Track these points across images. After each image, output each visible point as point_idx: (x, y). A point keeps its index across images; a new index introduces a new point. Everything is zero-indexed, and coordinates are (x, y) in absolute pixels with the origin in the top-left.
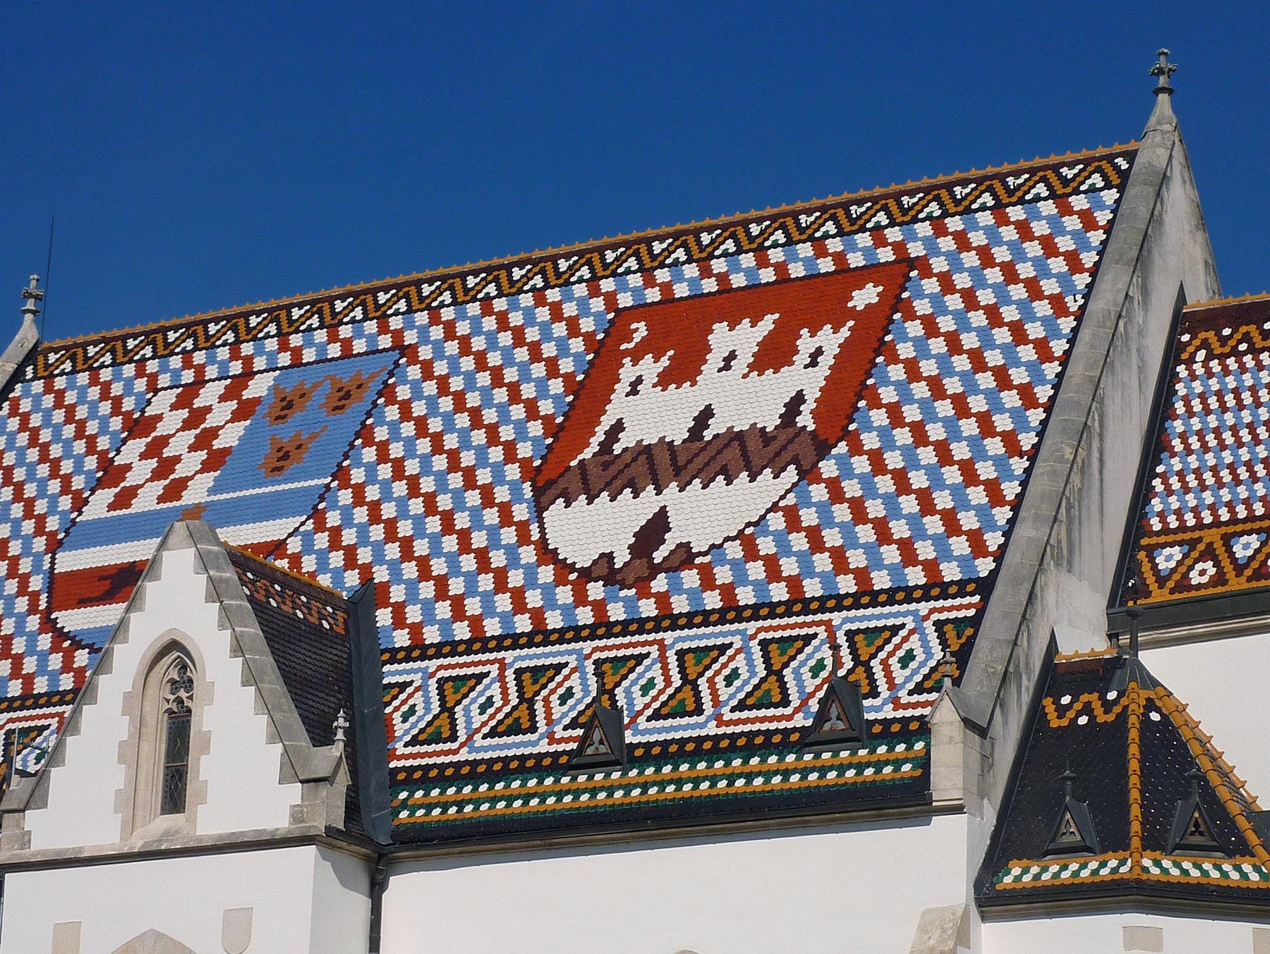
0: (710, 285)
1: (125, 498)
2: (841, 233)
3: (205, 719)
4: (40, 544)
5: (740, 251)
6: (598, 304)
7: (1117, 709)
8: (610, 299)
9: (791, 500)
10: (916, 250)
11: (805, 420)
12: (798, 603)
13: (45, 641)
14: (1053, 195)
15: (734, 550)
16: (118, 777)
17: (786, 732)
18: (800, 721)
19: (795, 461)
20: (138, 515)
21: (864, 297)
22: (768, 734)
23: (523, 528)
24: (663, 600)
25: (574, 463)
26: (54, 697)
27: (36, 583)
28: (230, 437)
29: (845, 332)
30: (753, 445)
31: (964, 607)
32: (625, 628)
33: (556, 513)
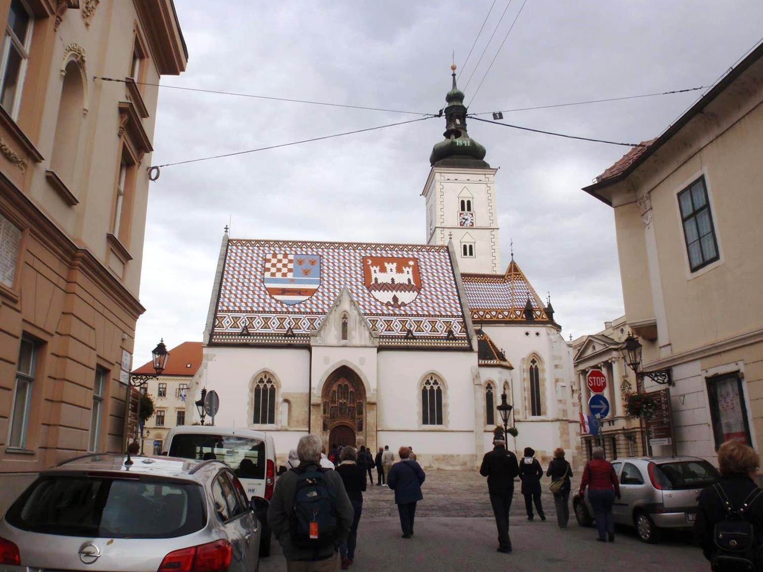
0: (379, 255)
1: (273, 274)
2: (399, 250)
3: (350, 325)
4: (258, 281)
5: (381, 250)
6: (357, 254)
7: (484, 337)
8: (359, 254)
9: (418, 297)
10: (416, 257)
11: (413, 283)
12: (429, 315)
13: (274, 301)
14: (436, 252)
15: (412, 304)
16: (336, 333)
17: (442, 337)
18: (442, 335)
19: (415, 290)
20: (277, 279)
21: (411, 263)
22: (436, 337)
23: (368, 294)
24: (404, 311)
25: (371, 284)
26: (283, 312)
27: (263, 289)
28: (291, 266)
29: (411, 269)
30: (406, 286)
31: (461, 320)
32: (401, 315)
33: (373, 292)
